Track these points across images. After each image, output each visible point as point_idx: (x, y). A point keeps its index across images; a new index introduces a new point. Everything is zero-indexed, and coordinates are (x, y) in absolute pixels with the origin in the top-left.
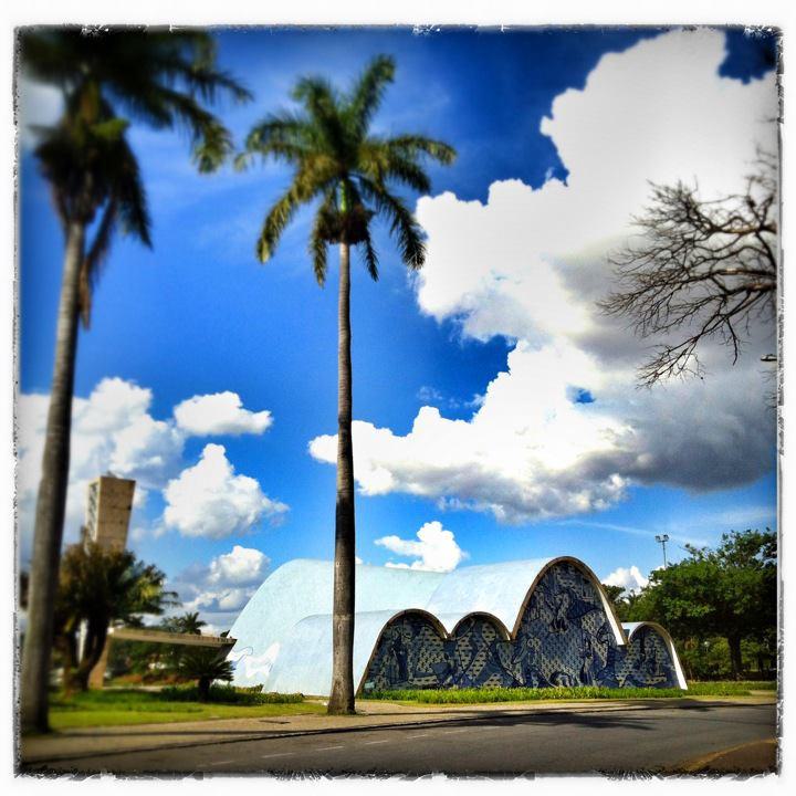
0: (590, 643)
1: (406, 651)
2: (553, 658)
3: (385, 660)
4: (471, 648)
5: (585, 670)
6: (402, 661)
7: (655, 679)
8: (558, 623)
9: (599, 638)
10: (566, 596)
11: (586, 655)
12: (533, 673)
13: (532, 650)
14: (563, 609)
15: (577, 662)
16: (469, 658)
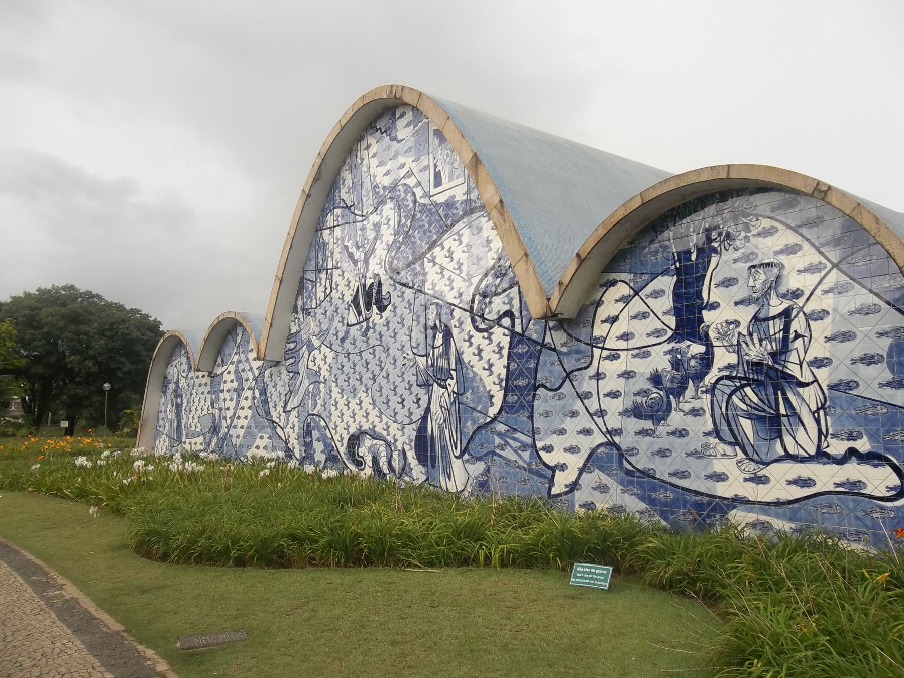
0: (448, 335)
1: (181, 397)
2: (354, 392)
3: (168, 412)
4: (235, 384)
5: (432, 427)
6: (178, 414)
7: (780, 472)
8: (368, 295)
9: (476, 316)
10: (388, 210)
11: (439, 376)
12: (315, 434)
13: (315, 377)
14: (381, 251)
15: (410, 400)
16: (232, 405)
